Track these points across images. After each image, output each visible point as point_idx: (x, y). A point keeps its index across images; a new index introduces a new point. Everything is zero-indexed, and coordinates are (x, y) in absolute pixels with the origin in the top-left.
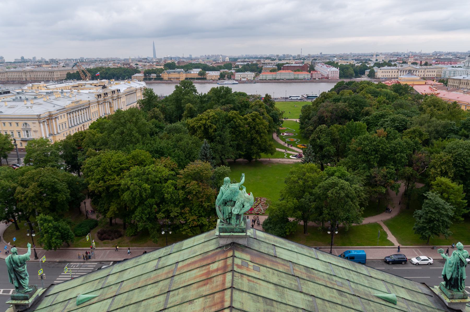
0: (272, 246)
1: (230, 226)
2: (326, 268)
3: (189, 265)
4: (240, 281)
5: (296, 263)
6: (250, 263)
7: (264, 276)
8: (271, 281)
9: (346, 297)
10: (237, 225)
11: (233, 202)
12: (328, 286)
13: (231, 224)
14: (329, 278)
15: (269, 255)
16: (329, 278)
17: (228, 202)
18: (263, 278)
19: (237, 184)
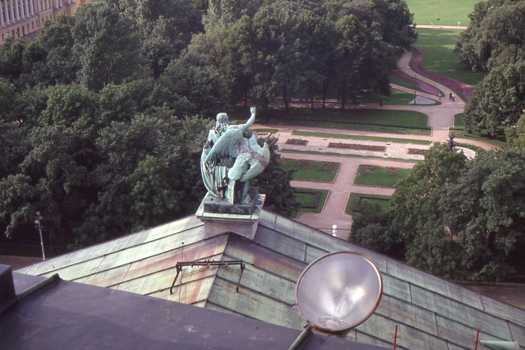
1: (223, 203)
2: (399, 290)
3: (148, 267)
4: (224, 292)
7: (272, 290)
8: (283, 299)
9: (422, 339)
12: (393, 318)
14: (399, 307)
15: (292, 258)
16: (399, 307)
18: (269, 293)
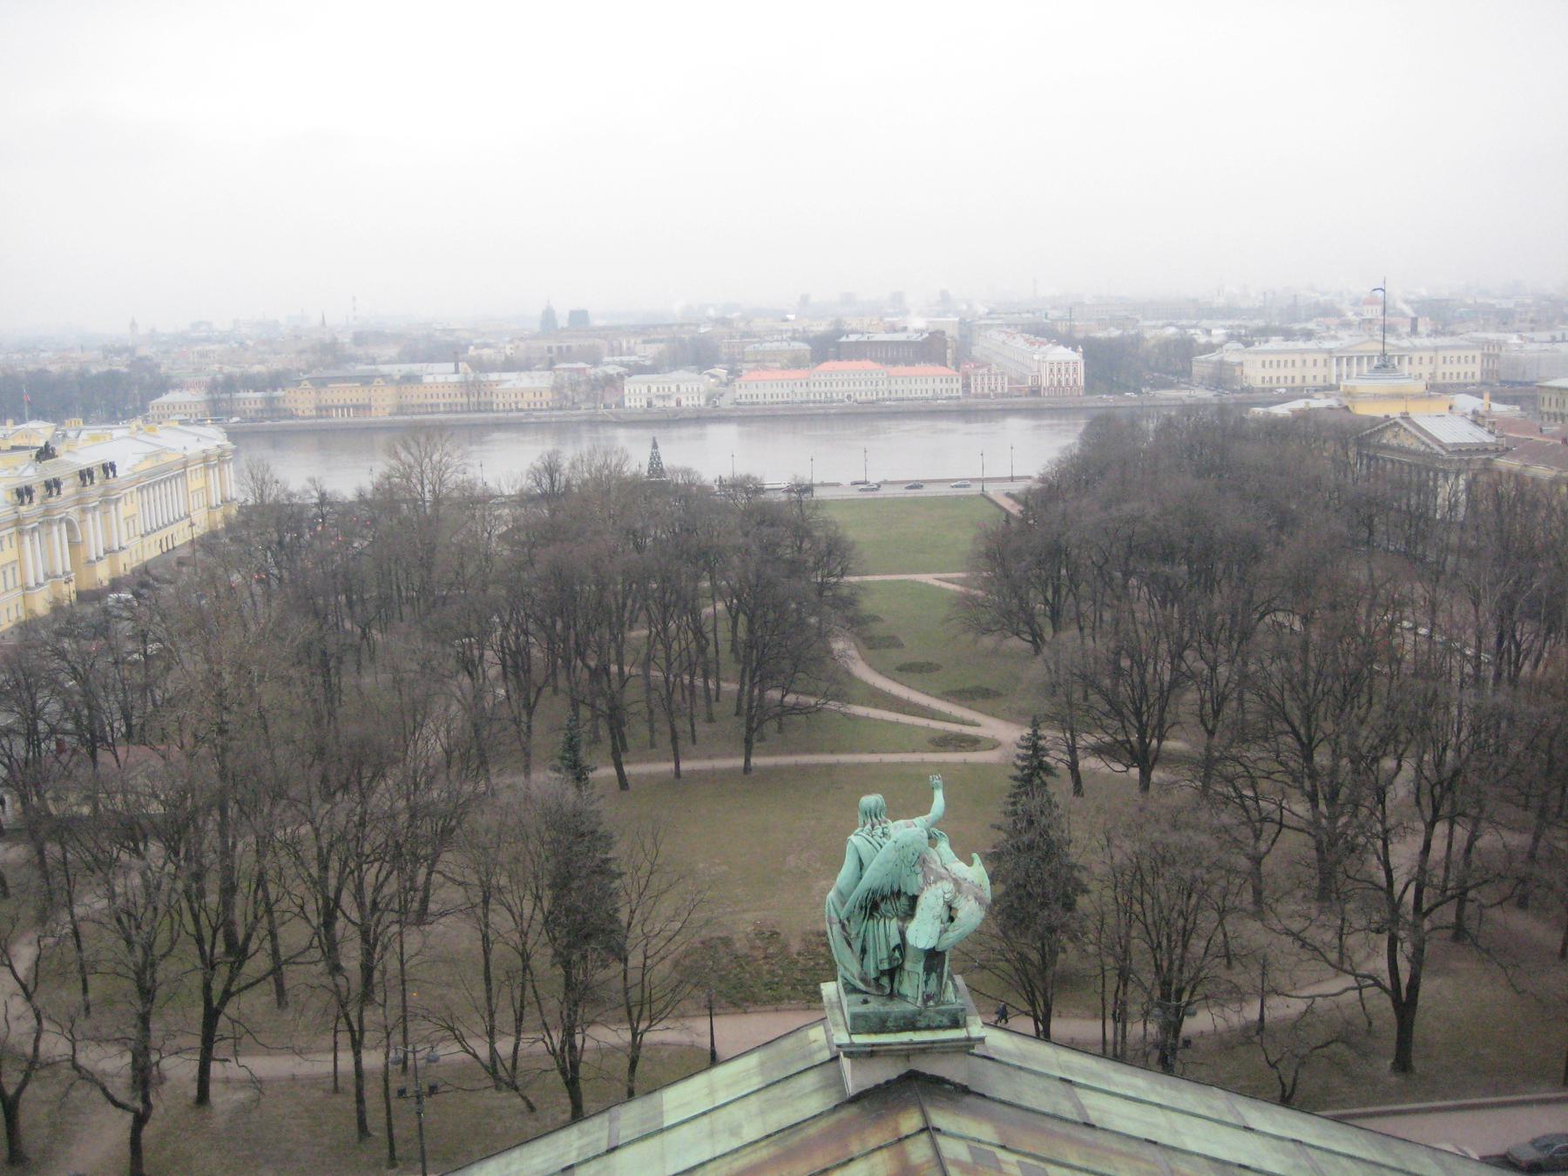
0: (1059, 1084)
1: (897, 1008)
5: (1174, 1149)
6: (1001, 1154)
10: (928, 998)
11: (903, 900)
13: (904, 997)
17: (884, 898)
19: (917, 820)
